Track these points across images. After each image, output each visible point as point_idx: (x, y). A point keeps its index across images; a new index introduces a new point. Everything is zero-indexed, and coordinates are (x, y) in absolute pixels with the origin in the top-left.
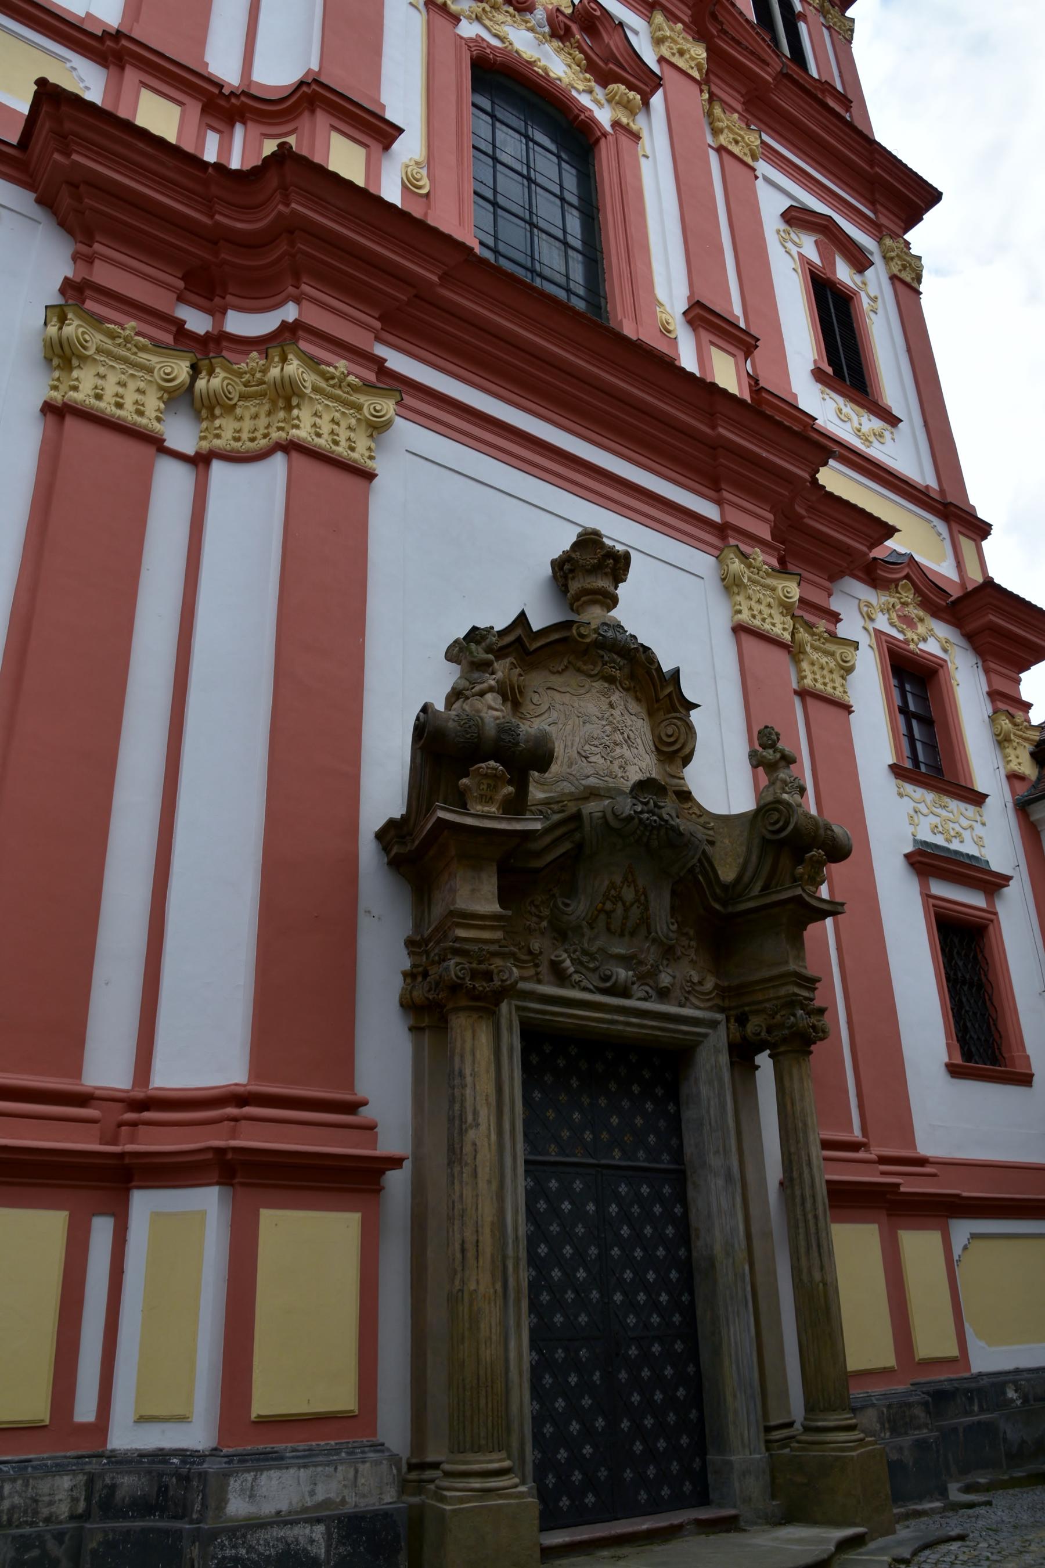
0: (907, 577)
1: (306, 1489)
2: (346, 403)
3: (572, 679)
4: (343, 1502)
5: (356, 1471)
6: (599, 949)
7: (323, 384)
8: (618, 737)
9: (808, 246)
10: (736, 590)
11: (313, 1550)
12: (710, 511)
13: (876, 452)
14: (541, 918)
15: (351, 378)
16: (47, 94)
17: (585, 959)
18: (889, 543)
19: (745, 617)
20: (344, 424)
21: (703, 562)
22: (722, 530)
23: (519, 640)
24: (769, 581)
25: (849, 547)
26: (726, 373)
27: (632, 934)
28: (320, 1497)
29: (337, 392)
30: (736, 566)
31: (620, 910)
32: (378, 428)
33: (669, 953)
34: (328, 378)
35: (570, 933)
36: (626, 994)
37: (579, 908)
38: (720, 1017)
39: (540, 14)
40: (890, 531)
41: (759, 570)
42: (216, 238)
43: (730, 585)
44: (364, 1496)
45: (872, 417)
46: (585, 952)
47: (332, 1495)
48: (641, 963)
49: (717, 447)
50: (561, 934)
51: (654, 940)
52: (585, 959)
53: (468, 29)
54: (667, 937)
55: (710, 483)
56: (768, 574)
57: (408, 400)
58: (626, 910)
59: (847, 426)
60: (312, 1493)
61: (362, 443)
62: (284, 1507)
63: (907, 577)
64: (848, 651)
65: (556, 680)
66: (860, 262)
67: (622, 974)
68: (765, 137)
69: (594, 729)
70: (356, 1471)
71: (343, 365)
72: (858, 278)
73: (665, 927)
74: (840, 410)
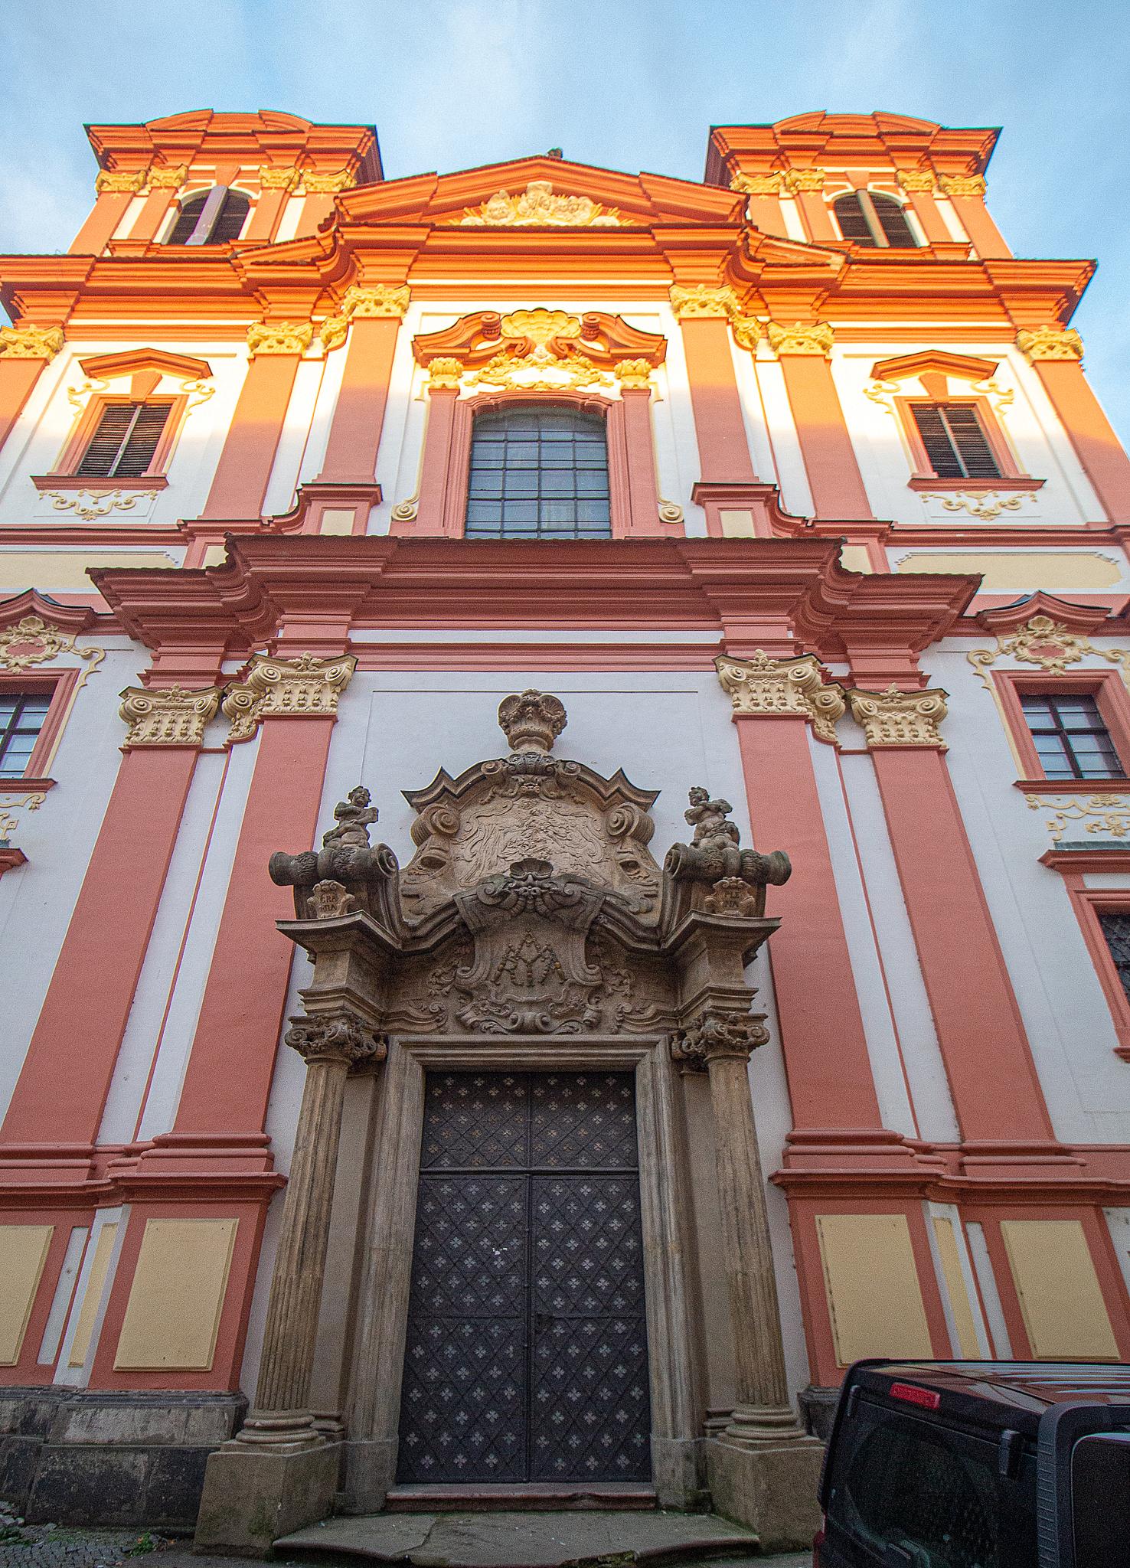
0: (1040, 612)
1: (139, 1425)
2: (313, 678)
3: (498, 803)
4: (172, 1438)
5: (189, 1415)
6: (508, 1000)
7: (293, 671)
8: (541, 835)
9: (912, 387)
10: (732, 690)
11: (135, 1473)
12: (714, 637)
13: (1008, 519)
14: (443, 985)
15: (315, 660)
16: (97, 575)
17: (494, 1009)
18: (981, 591)
19: (746, 707)
20: (312, 691)
21: (703, 681)
22: (721, 648)
23: (445, 789)
24: (779, 671)
25: (922, 611)
26: (741, 523)
27: (542, 983)
28: (151, 1432)
29: (306, 672)
30: (727, 670)
31: (522, 967)
32: (341, 686)
33: (596, 991)
34: (296, 666)
35: (475, 993)
36: (537, 1031)
37: (480, 970)
38: (655, 1037)
39: (541, 349)
40: (974, 581)
41: (764, 666)
42: (230, 613)
43: (729, 686)
44: (193, 1435)
45: (998, 493)
46: (493, 1004)
47: (163, 1432)
48: (560, 1005)
49: (699, 586)
50: (467, 994)
51: (571, 985)
52: (494, 1009)
53: (467, 393)
54: (585, 980)
55: (711, 613)
56: (776, 666)
57: (361, 658)
58: (529, 964)
59: (963, 512)
60: (144, 1429)
61: (328, 697)
62: (117, 1437)
63: (1040, 612)
64: (935, 702)
65: (484, 810)
66: (983, 370)
67: (529, 1015)
68: (834, 325)
69: (515, 836)
70: (189, 1415)
71: (305, 654)
72: (984, 385)
73: (581, 973)
74: (950, 503)
